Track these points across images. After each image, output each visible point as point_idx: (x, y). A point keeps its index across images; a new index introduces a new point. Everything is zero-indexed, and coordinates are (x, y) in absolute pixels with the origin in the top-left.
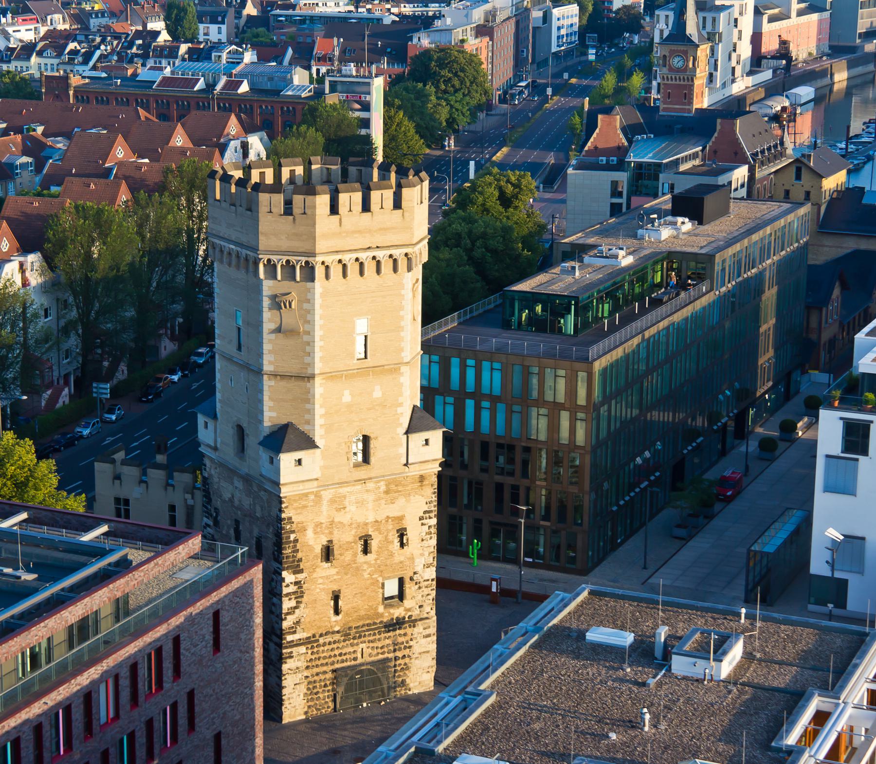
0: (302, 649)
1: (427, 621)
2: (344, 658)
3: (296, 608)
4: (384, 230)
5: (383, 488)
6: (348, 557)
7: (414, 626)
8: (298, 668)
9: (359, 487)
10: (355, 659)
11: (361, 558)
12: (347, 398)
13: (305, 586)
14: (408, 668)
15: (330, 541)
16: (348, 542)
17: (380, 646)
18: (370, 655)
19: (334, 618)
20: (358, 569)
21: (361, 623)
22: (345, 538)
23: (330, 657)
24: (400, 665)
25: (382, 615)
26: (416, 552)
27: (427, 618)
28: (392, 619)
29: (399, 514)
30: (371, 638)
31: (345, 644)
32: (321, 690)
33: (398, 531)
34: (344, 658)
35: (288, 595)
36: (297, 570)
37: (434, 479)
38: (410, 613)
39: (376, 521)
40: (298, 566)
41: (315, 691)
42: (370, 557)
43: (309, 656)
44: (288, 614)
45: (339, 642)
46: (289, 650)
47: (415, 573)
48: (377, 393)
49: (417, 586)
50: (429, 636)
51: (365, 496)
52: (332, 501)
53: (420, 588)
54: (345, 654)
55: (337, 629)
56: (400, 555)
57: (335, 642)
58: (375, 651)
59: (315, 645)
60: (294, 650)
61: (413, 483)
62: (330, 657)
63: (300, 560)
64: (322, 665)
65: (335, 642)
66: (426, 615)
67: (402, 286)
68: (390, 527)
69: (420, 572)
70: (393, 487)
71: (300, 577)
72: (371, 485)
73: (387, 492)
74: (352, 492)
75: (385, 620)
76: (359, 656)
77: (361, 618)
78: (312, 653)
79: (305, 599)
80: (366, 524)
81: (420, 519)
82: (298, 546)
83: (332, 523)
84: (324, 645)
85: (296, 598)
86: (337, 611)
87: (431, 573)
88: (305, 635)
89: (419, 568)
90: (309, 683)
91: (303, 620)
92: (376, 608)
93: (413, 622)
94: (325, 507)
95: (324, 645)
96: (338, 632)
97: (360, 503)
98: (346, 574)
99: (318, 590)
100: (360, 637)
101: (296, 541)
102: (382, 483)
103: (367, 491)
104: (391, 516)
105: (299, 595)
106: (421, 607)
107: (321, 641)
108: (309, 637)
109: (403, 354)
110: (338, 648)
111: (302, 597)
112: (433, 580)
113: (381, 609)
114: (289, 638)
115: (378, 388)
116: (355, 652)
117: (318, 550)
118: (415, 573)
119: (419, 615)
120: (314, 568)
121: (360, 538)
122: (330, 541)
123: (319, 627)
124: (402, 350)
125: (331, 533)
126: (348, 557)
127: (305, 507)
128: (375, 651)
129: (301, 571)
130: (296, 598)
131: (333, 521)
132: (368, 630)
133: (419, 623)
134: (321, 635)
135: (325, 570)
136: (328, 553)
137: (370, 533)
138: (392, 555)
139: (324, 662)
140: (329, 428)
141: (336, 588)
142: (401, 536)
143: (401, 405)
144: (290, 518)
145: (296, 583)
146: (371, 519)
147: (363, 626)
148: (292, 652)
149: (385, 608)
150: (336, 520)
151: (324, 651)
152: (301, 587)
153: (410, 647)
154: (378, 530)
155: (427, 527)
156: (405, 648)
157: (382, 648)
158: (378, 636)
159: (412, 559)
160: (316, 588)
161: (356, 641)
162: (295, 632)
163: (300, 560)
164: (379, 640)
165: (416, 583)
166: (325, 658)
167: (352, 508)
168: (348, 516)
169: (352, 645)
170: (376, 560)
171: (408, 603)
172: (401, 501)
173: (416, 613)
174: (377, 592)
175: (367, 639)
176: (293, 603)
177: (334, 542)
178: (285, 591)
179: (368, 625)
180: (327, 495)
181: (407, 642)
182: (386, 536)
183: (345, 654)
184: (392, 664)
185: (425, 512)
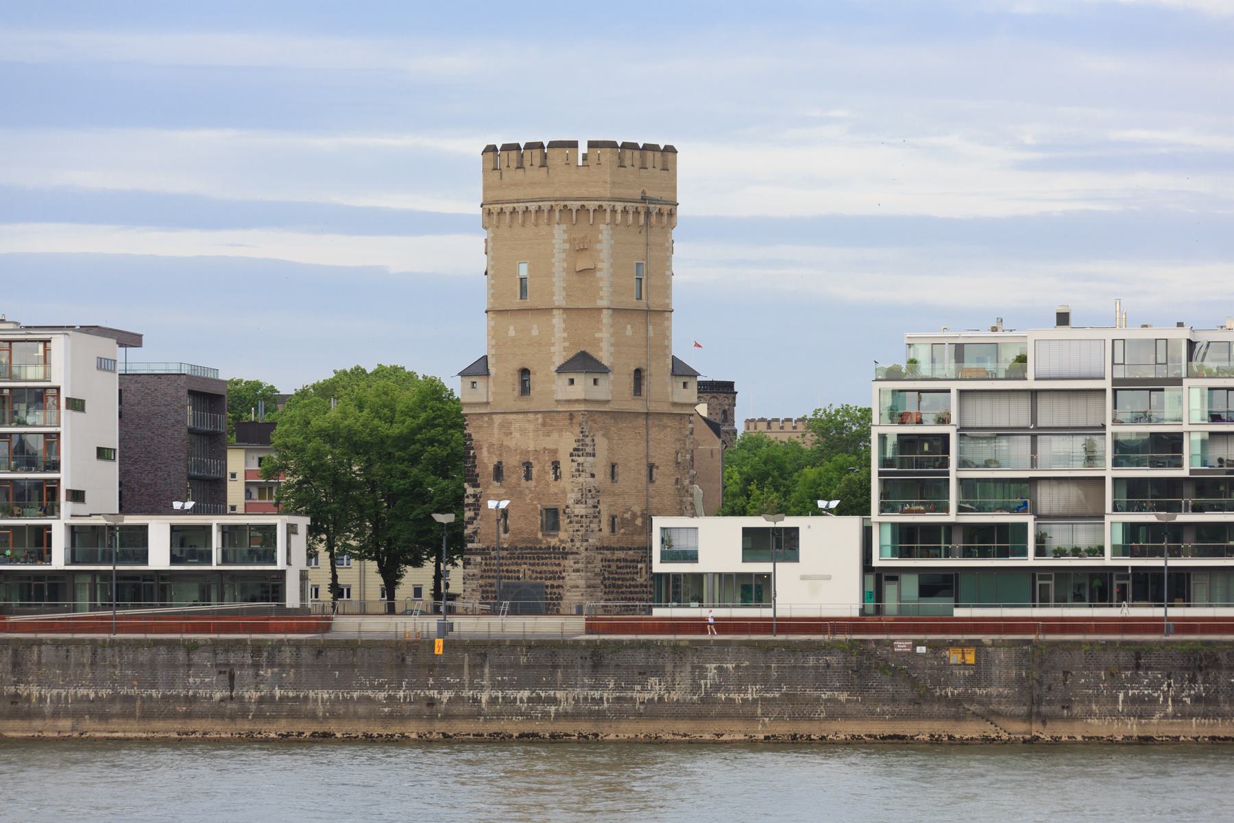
0: (479, 559)
3: (475, 518)
5: (540, 420)
6: (513, 479)
9: (521, 416)
11: (523, 480)
12: (512, 333)
15: (500, 463)
18: (530, 577)
19: (503, 536)
25: (541, 542)
26: (569, 487)
29: (553, 447)
35: (468, 505)
36: (476, 485)
42: (532, 483)
43: (484, 567)
44: (468, 523)
50: (577, 571)
52: (502, 426)
55: (505, 546)
60: (472, 557)
63: (477, 475)
66: (575, 549)
67: (553, 236)
71: (478, 490)
72: (531, 416)
73: (544, 424)
74: (517, 422)
77: (524, 540)
79: (481, 512)
81: (571, 455)
82: (477, 462)
88: (480, 546)
89: (570, 502)
90: (483, 592)
93: (565, 554)
94: (496, 431)
96: (507, 549)
97: (523, 432)
101: (475, 457)
102: (540, 416)
106: (572, 541)
107: (493, 553)
109: (555, 298)
113: (540, 535)
114: (470, 546)
115: (535, 326)
117: (491, 468)
120: (488, 484)
122: (500, 463)
124: (553, 294)
125: (501, 455)
127: (481, 427)
129: (477, 486)
133: (570, 556)
135: (495, 487)
136: (498, 472)
138: (548, 485)
143: (553, 344)
144: (470, 435)
145: (475, 496)
146: (531, 448)
147: (527, 548)
154: (537, 459)
156: (559, 578)
159: (564, 492)
162: (473, 542)
163: (477, 475)
166: (495, 571)
167: (517, 435)
168: (514, 443)
169: (517, 564)
171: (562, 535)
172: (555, 435)
173: (568, 545)
178: (467, 501)
179: (531, 548)
180: (497, 419)
184: (549, 591)
185: (575, 450)
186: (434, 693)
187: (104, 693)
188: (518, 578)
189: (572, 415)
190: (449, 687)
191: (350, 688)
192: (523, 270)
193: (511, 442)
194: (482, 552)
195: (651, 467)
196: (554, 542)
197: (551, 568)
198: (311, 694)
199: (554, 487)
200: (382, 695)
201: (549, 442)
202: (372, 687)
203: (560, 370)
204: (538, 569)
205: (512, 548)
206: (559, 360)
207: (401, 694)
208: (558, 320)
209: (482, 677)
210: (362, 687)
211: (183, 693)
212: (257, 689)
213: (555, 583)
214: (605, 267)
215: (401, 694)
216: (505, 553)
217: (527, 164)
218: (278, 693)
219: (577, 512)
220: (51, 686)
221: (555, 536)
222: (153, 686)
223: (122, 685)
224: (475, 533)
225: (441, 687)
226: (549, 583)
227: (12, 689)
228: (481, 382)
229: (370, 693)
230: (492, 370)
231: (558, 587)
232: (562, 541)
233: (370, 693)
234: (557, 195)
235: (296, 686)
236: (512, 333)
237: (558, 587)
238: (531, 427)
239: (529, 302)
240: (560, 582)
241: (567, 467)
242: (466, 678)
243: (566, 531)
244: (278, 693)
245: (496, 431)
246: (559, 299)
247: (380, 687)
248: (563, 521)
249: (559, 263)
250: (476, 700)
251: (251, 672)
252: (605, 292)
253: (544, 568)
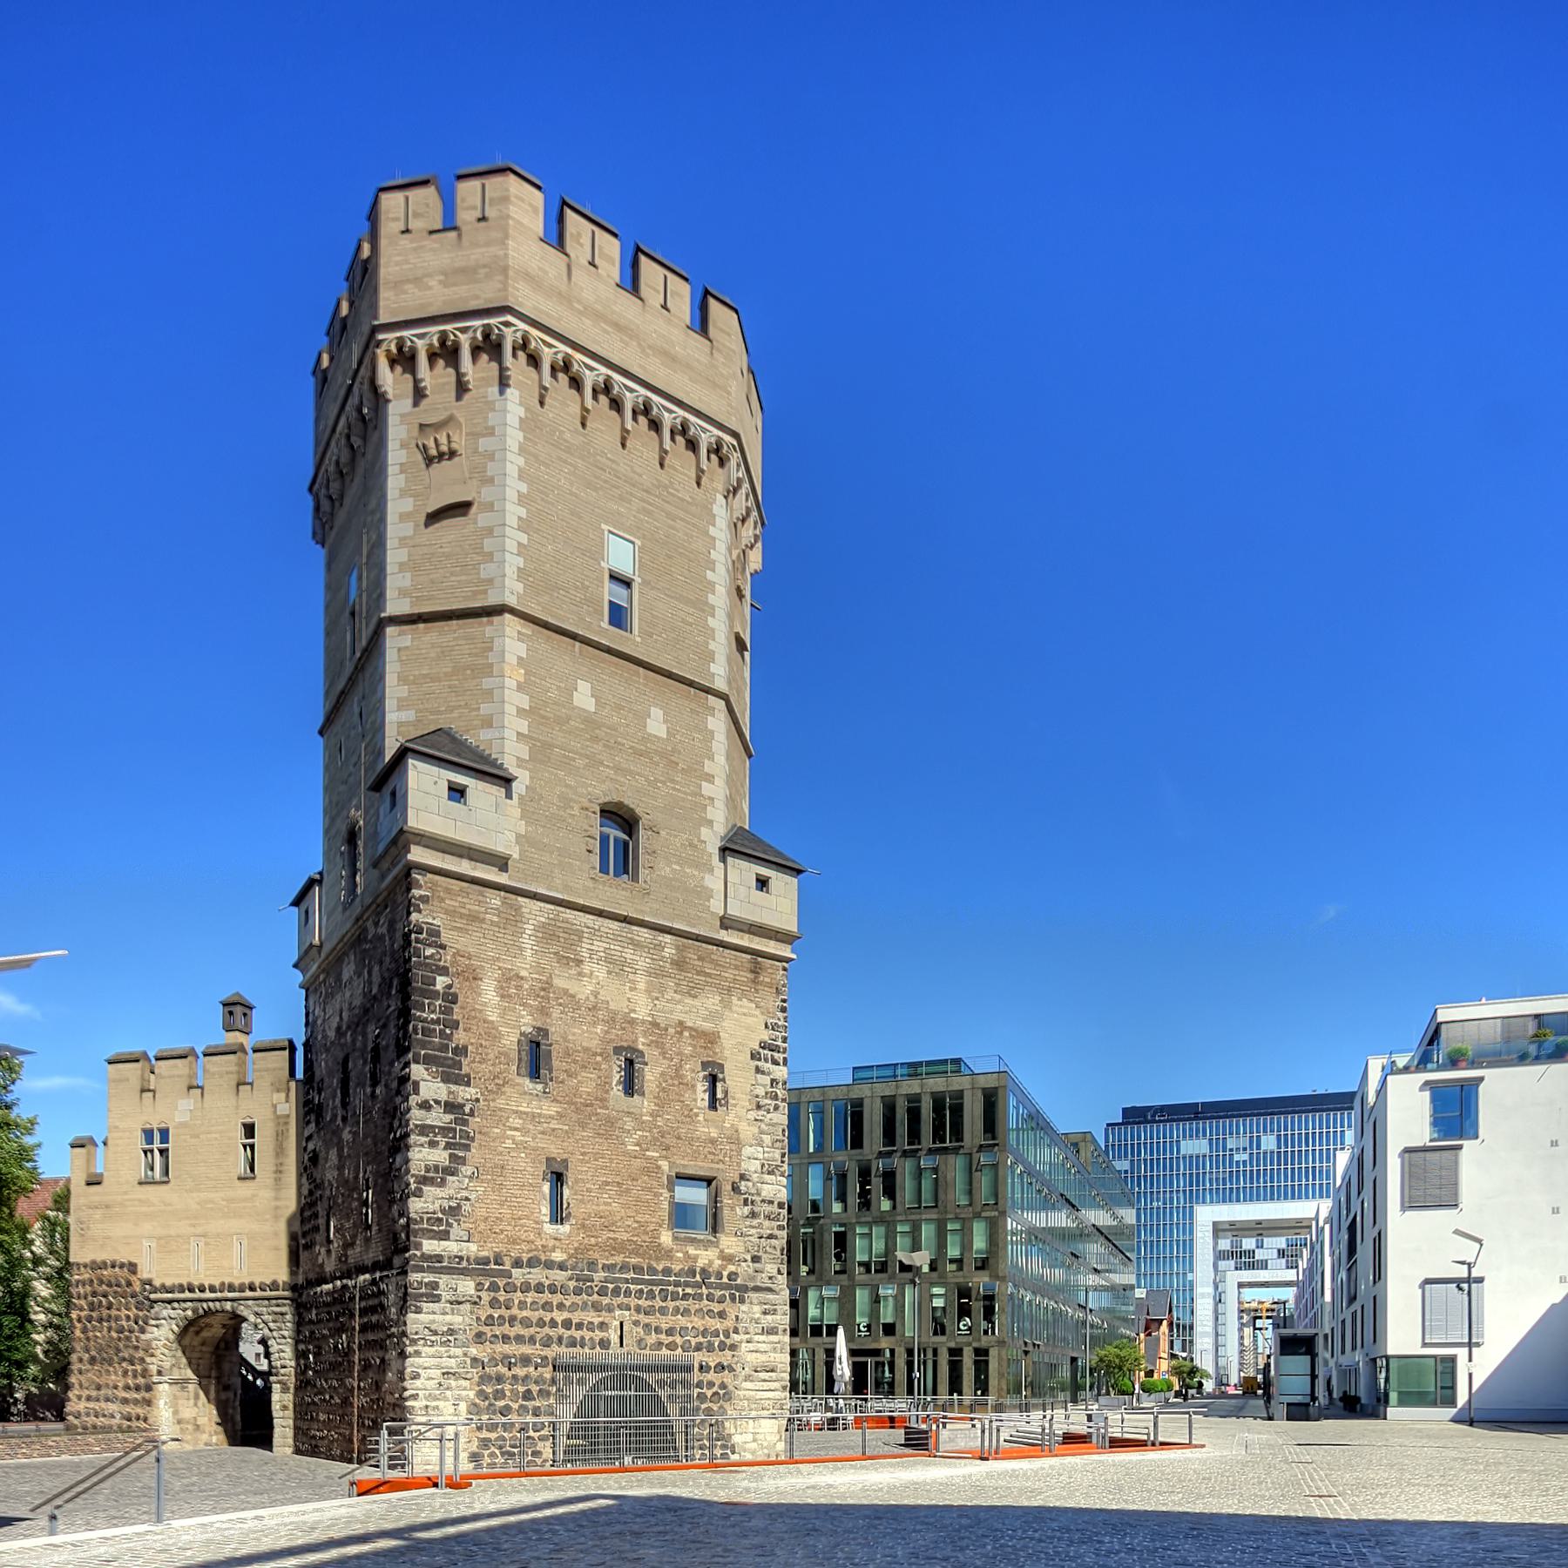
0: (467, 1286)
1: (771, 1296)
2: (578, 1334)
7: (742, 1301)
8: (451, 1332)
9: (615, 925)
10: (604, 1344)
13: (475, 1121)
14: (728, 1397)
15: (542, 1031)
16: (586, 1050)
17: (664, 1326)
19: (549, 1228)
20: (611, 1122)
21: (619, 1259)
22: (575, 1035)
23: (541, 1323)
24: (711, 1384)
25: (668, 1254)
26: (747, 1131)
27: (770, 1290)
28: (692, 1273)
30: (643, 1303)
31: (577, 1299)
32: (515, 1406)
33: (705, 1065)
34: (578, 1334)
38: (732, 1268)
39: (655, 1025)
40: (459, 1065)
41: (501, 1403)
42: (644, 1105)
45: (563, 1290)
46: (429, 1278)
47: (742, 1177)
49: (746, 1210)
51: (629, 954)
53: (753, 1215)
54: (579, 1326)
55: (558, 1256)
56: (706, 1126)
57: (553, 1289)
58: (652, 1338)
59: (501, 1283)
60: (443, 1280)
61: (736, 968)
62: (541, 1323)
63: (461, 1051)
64: (519, 1339)
65: (553, 1289)
68: (688, 1050)
69: (755, 1177)
70: (692, 956)
71: (465, 1093)
73: (680, 964)
74: (599, 938)
75: (676, 1267)
76: (614, 1337)
77: (618, 1247)
78: (494, 1303)
80: (632, 1022)
81: (753, 1057)
83: (547, 986)
84: (526, 1288)
85: (448, 1146)
86: (558, 1216)
87: (776, 1189)
88: (472, 1249)
91: (466, 1207)
92: (655, 1235)
93: (739, 1292)
95: (526, 1288)
96: (562, 1266)
98: (583, 1126)
99: (509, 1144)
100: (616, 1292)
103: (636, 945)
104: (689, 1024)
105: (458, 1140)
106: (756, 1259)
108: (486, 1261)
110: (561, 1306)
111: (467, 1148)
112: (781, 1206)
113: (666, 1238)
114: (429, 1246)
116: (603, 1326)
117: (510, 1040)
118: (742, 1177)
119: (753, 1279)
120: (499, 1085)
121: (618, 1050)
123: (514, 1241)
125: (543, 1011)
126: (587, 1084)
128: (652, 1338)
130: (448, 1146)
131: (549, 983)
132: (634, 1282)
133: (754, 1296)
134: (517, 1263)
136: (536, 1057)
137: (641, 1047)
138: (691, 1116)
139: (526, 1332)
141: (555, 1150)
142: (713, 1080)
145: (450, 1107)
147: (624, 1267)
148: (435, 1286)
149: (675, 1238)
150: (559, 982)
152: (465, 1123)
153: (733, 1347)
154: (657, 1044)
155: (767, 1080)
157: (670, 1332)
158: (658, 1303)
160: (504, 1137)
161: (606, 1301)
162: (444, 1236)
163: (461, 1051)
164: (663, 1311)
165: (746, 1202)
166: (526, 1323)
169: (597, 1307)
170: (653, 1115)
171: (729, 1243)
172: (712, 1001)
173: (745, 1269)
174: (657, 1195)
175: (633, 1301)
176: (440, 1156)
177: (553, 1037)
181: (728, 1336)
182: (679, 1068)
183: (579, 1326)
188: (604, 1344)
194: (480, 1268)
196: (706, 1257)
197: (699, 1323)
199: (706, 1126)
201: (698, 1010)
204: (665, 1322)
205: (582, 1269)
213: (712, 1360)
216: (559, 1276)
219: (767, 1191)
221: (707, 1245)
224: (454, 1211)
226: (698, 1358)
231: (721, 1367)
232: (728, 1259)
237: (721, 1367)
238: (642, 963)
240: (726, 1357)
241: (740, 1080)
243: (740, 1234)
245: (528, 942)
248: (734, 1213)
253: (682, 1321)
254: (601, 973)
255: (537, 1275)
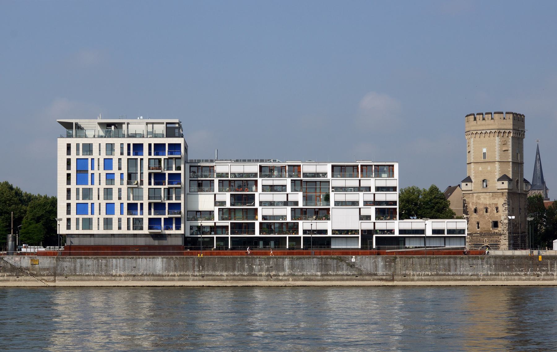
4: (489, 125)
6: (481, 212)
12: (480, 169)
25: (491, 231)
26: (502, 215)
36: (467, 214)
37: (506, 194)
42: (488, 214)
48: (489, 169)
52: (477, 197)
56: (496, 215)
73: (492, 196)
77: (485, 231)
86: (478, 228)
93: (501, 235)
97: (485, 198)
113: (491, 229)
117: (473, 209)
126: (481, 212)
135: (474, 215)
136: (476, 211)
140: (475, 177)
142: (497, 209)
146: (488, 203)
151: (475, 238)
159: (500, 216)
167: (482, 199)
171: (499, 229)
172: (497, 199)
186: (539, 273)
187: (433, 273)
189: (503, 193)
190: (544, 271)
191: (512, 271)
192: (485, 150)
193: (481, 202)
195: (520, 209)
196: (496, 231)
198: (500, 273)
199: (496, 215)
200: (523, 273)
201: (495, 201)
202: (519, 271)
203: (499, 180)
205: (481, 234)
206: (498, 177)
207: (529, 273)
208: (497, 165)
209: (554, 267)
210: (516, 271)
211: (459, 273)
212: (482, 272)
214: (510, 149)
215: (529, 273)
217: (477, 119)
218: (489, 273)
220: (416, 271)
222: (449, 271)
223: (440, 270)
225: (541, 271)
227: (404, 272)
228: (469, 184)
229: (519, 273)
230: (473, 180)
233: (519, 273)
234: (497, 128)
235: (496, 270)
236: (480, 169)
239: (487, 160)
241: (501, 209)
242: (549, 268)
244: (489, 273)
246: (497, 159)
247: (522, 271)
249: (497, 148)
250: (553, 275)
251: (481, 266)
252: (511, 157)
254: (482, 199)
255: (476, 235)
